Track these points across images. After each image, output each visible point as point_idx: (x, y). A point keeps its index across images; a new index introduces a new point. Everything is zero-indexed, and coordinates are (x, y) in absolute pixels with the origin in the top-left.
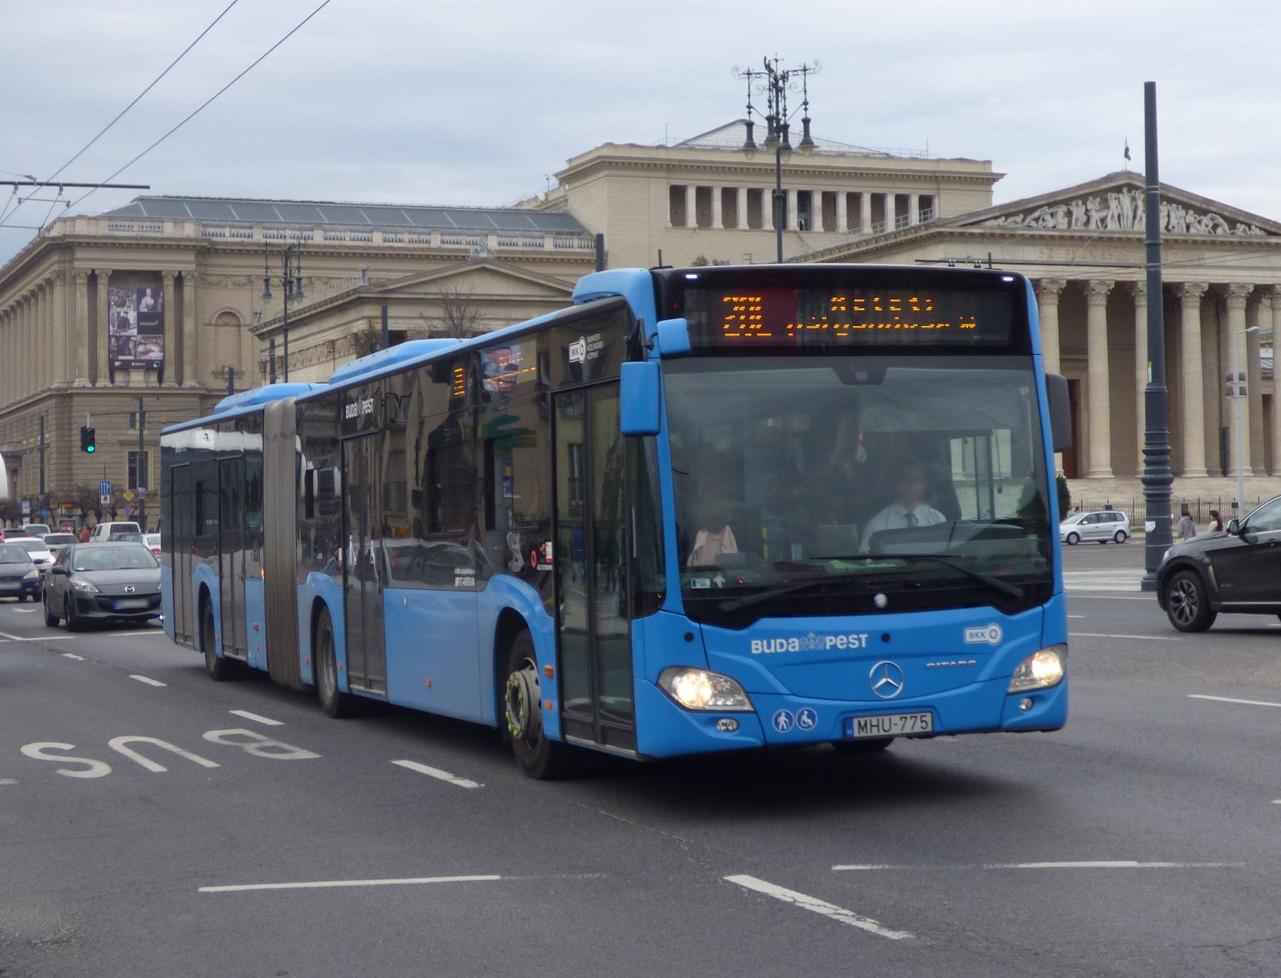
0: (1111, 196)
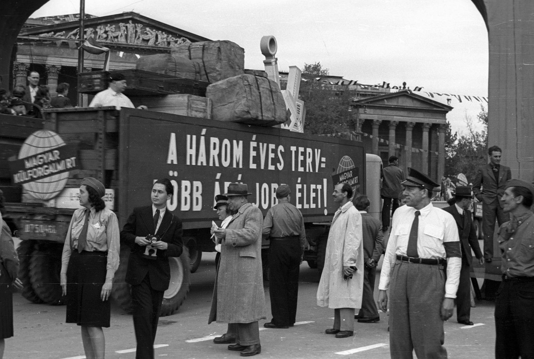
0: (121, 24)
